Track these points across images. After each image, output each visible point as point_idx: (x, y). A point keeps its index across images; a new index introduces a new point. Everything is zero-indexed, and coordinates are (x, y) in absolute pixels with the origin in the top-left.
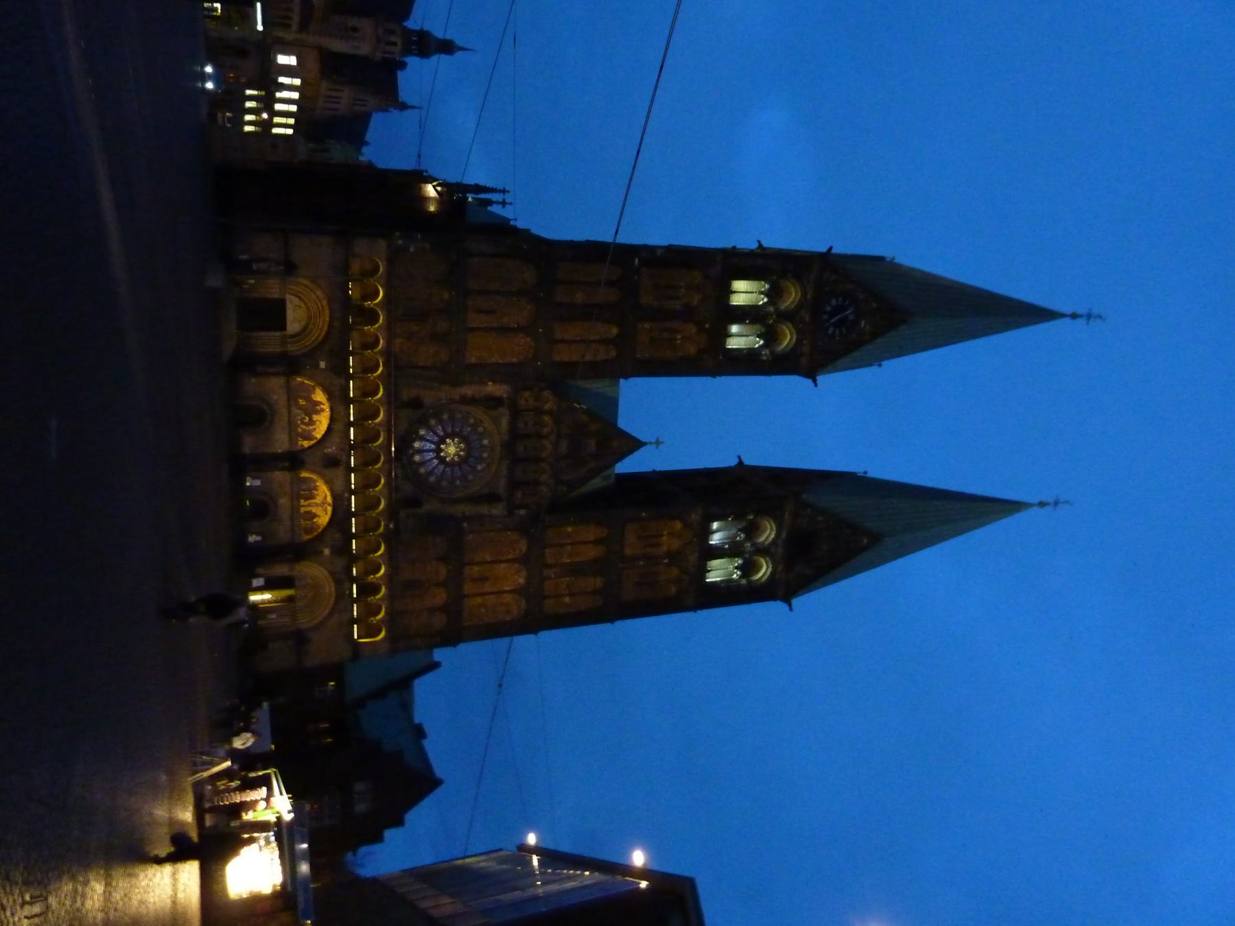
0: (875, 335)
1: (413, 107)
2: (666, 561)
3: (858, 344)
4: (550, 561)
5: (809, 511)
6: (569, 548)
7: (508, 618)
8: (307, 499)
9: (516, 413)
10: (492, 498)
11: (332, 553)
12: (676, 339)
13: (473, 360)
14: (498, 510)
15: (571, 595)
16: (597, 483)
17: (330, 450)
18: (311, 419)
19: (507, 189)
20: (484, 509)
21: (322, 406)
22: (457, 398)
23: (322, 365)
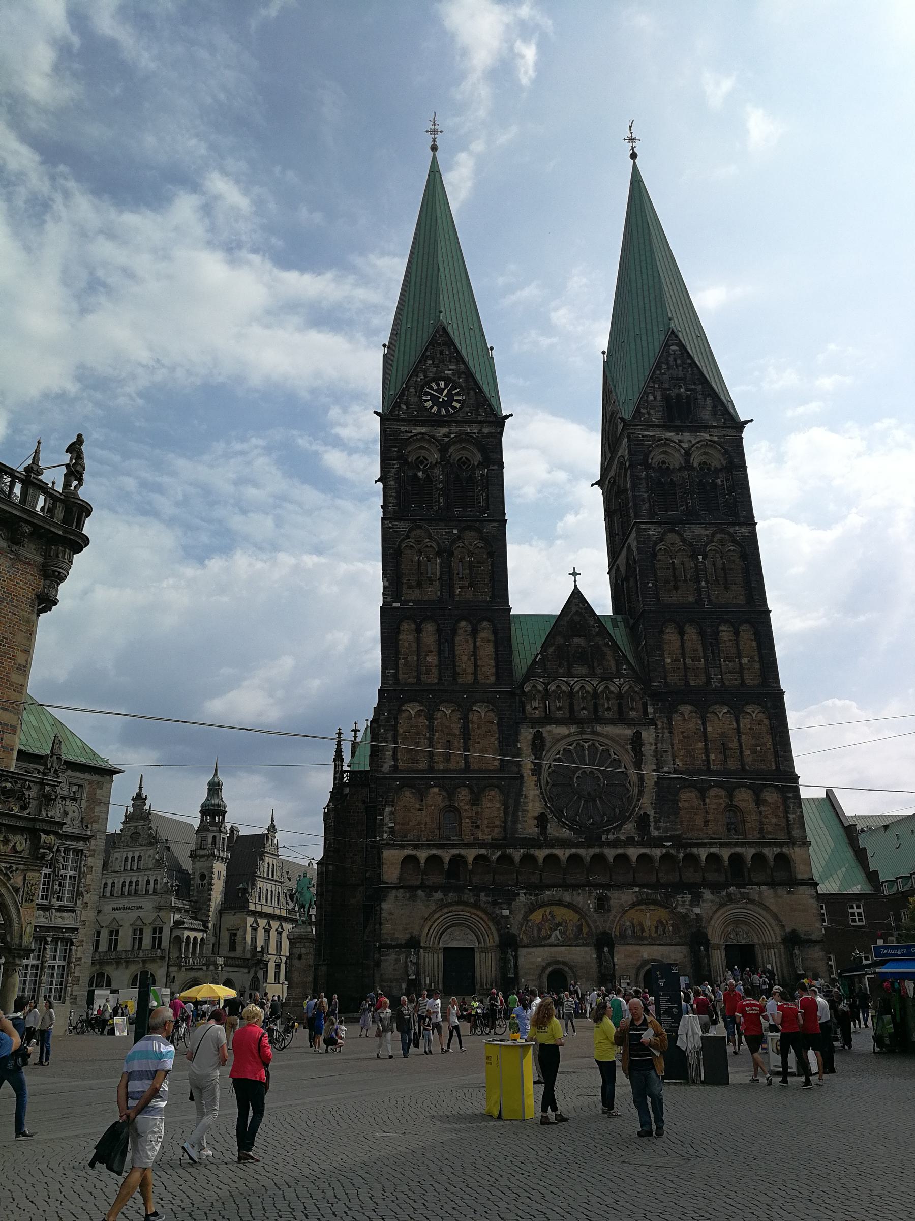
0: (460, 359)
1: (272, 820)
2: (700, 557)
3: (469, 375)
4: (703, 679)
5: (643, 411)
6: (688, 660)
7: (766, 722)
8: (643, 930)
9: (548, 719)
10: (637, 742)
11: (698, 905)
12: (470, 562)
14: (648, 735)
15: (739, 657)
16: (619, 635)
17: (591, 906)
18: (560, 924)
19: (338, 731)
20: (648, 750)
21: (547, 913)
22: (535, 778)
23: (506, 912)
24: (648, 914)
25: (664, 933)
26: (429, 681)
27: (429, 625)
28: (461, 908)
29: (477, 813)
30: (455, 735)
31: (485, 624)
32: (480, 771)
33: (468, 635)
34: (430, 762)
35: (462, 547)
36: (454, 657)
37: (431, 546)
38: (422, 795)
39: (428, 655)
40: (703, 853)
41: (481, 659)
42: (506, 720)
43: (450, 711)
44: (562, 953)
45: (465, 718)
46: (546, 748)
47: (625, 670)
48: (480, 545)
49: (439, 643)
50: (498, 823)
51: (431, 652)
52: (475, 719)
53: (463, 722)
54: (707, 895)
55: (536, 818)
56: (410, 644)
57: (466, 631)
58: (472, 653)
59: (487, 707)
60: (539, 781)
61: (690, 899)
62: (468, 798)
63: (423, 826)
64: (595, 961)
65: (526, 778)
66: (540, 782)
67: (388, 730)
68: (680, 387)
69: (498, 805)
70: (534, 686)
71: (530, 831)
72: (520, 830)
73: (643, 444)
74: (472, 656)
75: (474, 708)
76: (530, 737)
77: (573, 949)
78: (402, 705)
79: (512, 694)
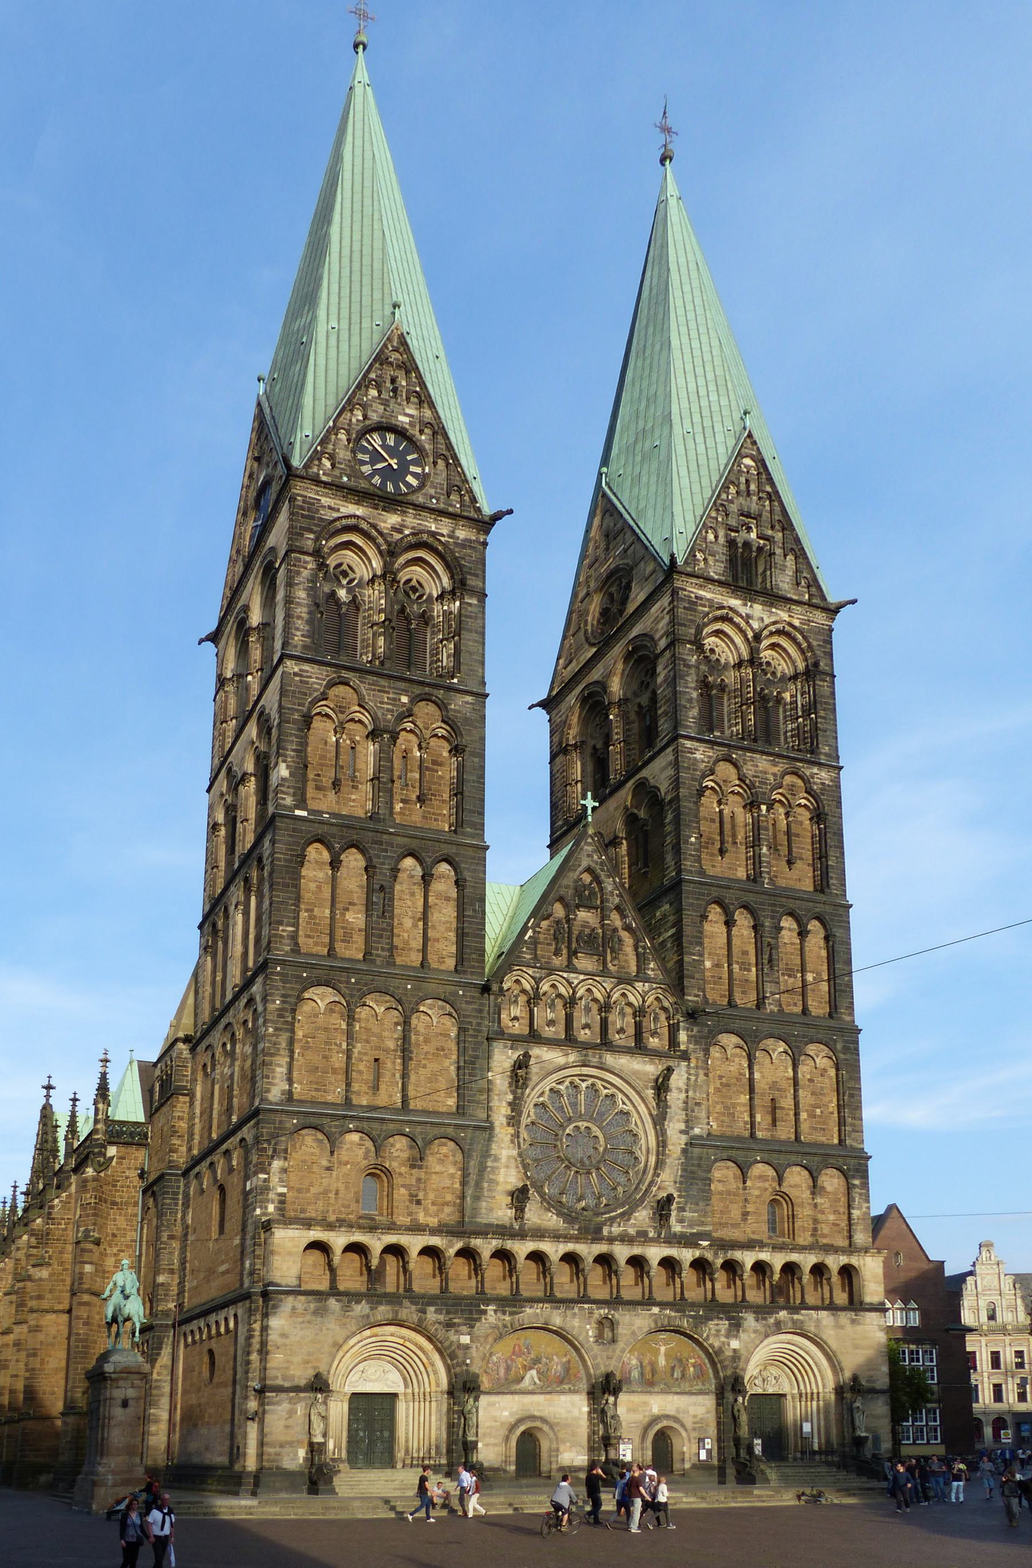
9: (534, 1037)
11: (736, 1337)
13: (452, 1102)
22: (511, 1130)
24: (663, 1349)
25: (683, 1376)
26: (348, 954)
27: (351, 858)
28: (392, 1329)
29: (419, 1180)
30: (387, 1050)
31: (444, 868)
32: (425, 1112)
33: (415, 884)
34: (347, 1091)
35: (411, 731)
36: (392, 918)
37: (360, 721)
38: (333, 1143)
39: (347, 909)
40: (748, 1259)
41: (434, 927)
42: (471, 1032)
43: (383, 1009)
44: (539, 1404)
45: (406, 1023)
46: (531, 1084)
47: (653, 970)
48: (441, 732)
49: (370, 891)
50: (449, 1197)
51: (354, 904)
52: (421, 1028)
53: (404, 1031)
54: (750, 1320)
55: (512, 1194)
56: (319, 887)
57: (412, 877)
58: (419, 915)
59: (443, 1008)
60: (517, 1135)
61: (727, 1326)
62: (405, 1155)
63: (332, 1195)
64: (586, 1416)
65: (497, 1130)
66: (518, 1137)
67: (280, 1029)
68: (749, 529)
69: (452, 1170)
70: (517, 981)
71: (500, 1213)
72: (483, 1211)
73: (695, 610)
74: (420, 919)
75: (422, 1009)
76: (508, 1064)
77: (555, 1397)
78: (305, 989)
79: (486, 989)
